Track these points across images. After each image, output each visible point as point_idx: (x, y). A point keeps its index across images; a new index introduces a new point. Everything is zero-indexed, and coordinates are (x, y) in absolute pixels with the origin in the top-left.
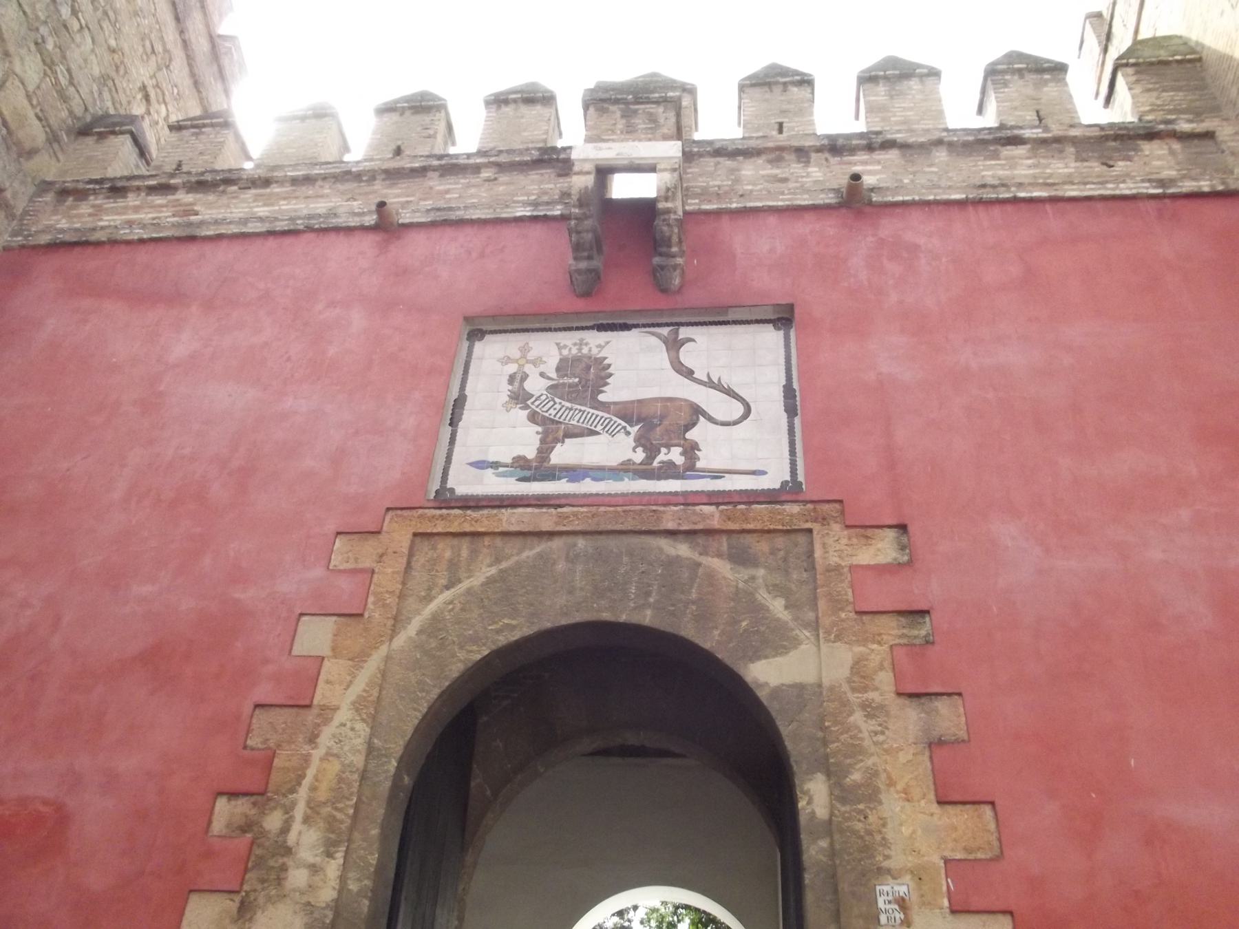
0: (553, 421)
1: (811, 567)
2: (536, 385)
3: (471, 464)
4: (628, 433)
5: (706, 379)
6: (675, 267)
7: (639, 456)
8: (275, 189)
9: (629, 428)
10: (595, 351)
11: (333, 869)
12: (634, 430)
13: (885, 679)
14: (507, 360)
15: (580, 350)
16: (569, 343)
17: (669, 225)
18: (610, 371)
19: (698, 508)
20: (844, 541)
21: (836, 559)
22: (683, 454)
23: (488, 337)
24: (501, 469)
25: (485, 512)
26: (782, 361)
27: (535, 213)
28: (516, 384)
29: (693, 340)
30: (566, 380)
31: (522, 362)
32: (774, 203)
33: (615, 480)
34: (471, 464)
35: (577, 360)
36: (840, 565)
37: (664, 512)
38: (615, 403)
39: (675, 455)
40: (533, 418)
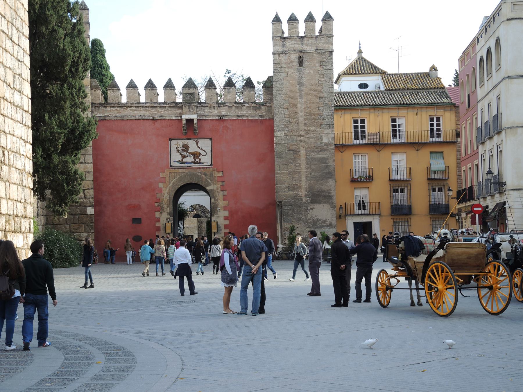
2: (180, 149)
7: (194, 160)
8: (132, 108)
11: (169, 209)
13: (220, 189)
14: (175, 145)
35: (185, 145)
39: (198, 160)
40: (180, 154)
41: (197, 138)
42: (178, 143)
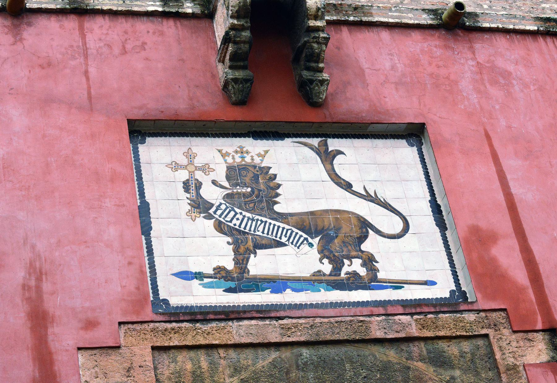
0: (239, 231)
1: (495, 366)
2: (211, 194)
3: (173, 275)
4: (311, 245)
5: (364, 193)
6: (322, 82)
7: (327, 267)
9: (310, 240)
10: (257, 160)
12: (315, 241)
14: (176, 167)
15: (243, 158)
16: (231, 150)
17: (318, 43)
18: (278, 180)
19: (396, 318)
20: (514, 344)
21: (512, 360)
22: (364, 265)
23: (149, 140)
24: (206, 280)
25: (214, 324)
26: (423, 177)
27: (167, 9)
28: (193, 192)
29: (342, 153)
30: (239, 189)
31: (191, 168)
32: (385, 20)
33: (313, 291)
34: (173, 275)
36: (516, 365)
37: (370, 322)
38: (291, 215)
40: (220, 227)
41: (321, 122)
42: (190, 156)
